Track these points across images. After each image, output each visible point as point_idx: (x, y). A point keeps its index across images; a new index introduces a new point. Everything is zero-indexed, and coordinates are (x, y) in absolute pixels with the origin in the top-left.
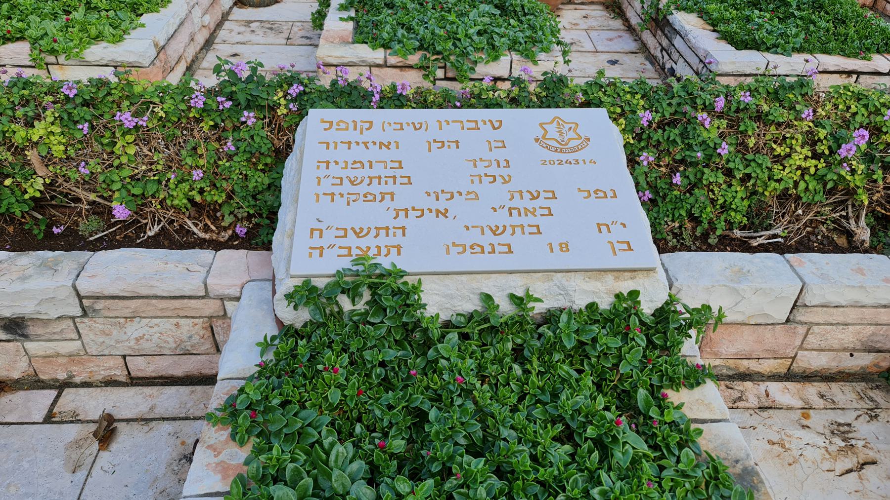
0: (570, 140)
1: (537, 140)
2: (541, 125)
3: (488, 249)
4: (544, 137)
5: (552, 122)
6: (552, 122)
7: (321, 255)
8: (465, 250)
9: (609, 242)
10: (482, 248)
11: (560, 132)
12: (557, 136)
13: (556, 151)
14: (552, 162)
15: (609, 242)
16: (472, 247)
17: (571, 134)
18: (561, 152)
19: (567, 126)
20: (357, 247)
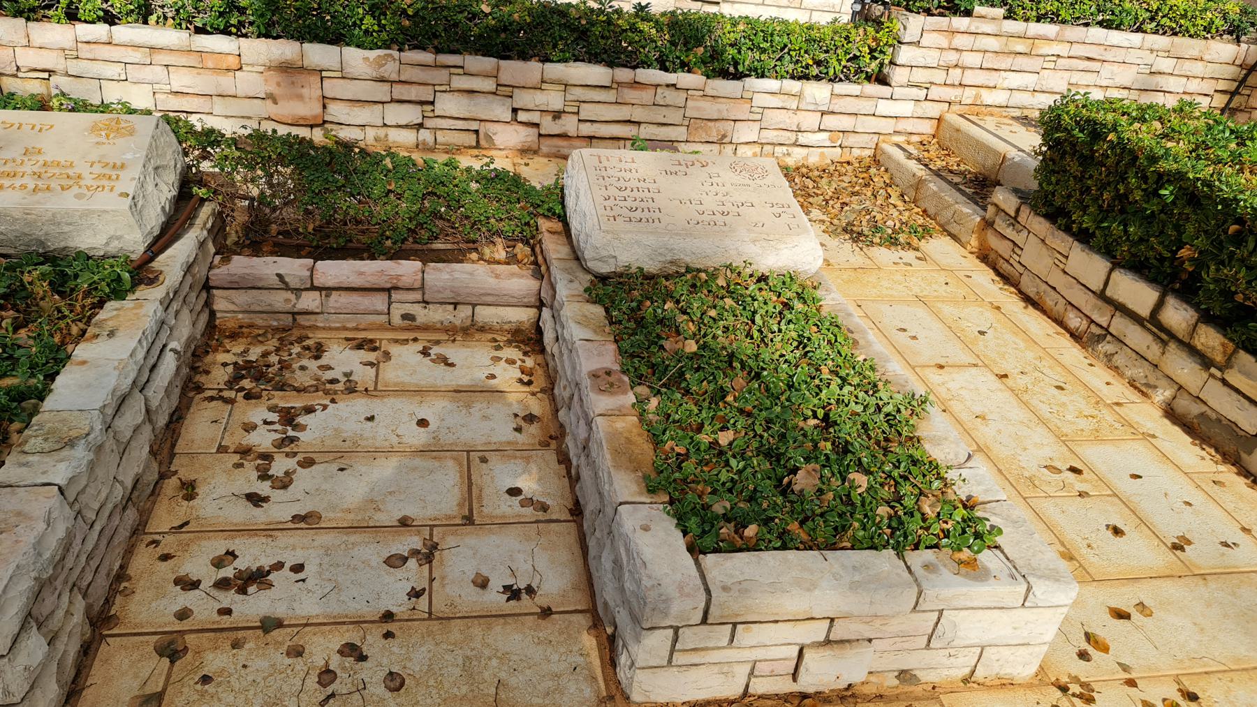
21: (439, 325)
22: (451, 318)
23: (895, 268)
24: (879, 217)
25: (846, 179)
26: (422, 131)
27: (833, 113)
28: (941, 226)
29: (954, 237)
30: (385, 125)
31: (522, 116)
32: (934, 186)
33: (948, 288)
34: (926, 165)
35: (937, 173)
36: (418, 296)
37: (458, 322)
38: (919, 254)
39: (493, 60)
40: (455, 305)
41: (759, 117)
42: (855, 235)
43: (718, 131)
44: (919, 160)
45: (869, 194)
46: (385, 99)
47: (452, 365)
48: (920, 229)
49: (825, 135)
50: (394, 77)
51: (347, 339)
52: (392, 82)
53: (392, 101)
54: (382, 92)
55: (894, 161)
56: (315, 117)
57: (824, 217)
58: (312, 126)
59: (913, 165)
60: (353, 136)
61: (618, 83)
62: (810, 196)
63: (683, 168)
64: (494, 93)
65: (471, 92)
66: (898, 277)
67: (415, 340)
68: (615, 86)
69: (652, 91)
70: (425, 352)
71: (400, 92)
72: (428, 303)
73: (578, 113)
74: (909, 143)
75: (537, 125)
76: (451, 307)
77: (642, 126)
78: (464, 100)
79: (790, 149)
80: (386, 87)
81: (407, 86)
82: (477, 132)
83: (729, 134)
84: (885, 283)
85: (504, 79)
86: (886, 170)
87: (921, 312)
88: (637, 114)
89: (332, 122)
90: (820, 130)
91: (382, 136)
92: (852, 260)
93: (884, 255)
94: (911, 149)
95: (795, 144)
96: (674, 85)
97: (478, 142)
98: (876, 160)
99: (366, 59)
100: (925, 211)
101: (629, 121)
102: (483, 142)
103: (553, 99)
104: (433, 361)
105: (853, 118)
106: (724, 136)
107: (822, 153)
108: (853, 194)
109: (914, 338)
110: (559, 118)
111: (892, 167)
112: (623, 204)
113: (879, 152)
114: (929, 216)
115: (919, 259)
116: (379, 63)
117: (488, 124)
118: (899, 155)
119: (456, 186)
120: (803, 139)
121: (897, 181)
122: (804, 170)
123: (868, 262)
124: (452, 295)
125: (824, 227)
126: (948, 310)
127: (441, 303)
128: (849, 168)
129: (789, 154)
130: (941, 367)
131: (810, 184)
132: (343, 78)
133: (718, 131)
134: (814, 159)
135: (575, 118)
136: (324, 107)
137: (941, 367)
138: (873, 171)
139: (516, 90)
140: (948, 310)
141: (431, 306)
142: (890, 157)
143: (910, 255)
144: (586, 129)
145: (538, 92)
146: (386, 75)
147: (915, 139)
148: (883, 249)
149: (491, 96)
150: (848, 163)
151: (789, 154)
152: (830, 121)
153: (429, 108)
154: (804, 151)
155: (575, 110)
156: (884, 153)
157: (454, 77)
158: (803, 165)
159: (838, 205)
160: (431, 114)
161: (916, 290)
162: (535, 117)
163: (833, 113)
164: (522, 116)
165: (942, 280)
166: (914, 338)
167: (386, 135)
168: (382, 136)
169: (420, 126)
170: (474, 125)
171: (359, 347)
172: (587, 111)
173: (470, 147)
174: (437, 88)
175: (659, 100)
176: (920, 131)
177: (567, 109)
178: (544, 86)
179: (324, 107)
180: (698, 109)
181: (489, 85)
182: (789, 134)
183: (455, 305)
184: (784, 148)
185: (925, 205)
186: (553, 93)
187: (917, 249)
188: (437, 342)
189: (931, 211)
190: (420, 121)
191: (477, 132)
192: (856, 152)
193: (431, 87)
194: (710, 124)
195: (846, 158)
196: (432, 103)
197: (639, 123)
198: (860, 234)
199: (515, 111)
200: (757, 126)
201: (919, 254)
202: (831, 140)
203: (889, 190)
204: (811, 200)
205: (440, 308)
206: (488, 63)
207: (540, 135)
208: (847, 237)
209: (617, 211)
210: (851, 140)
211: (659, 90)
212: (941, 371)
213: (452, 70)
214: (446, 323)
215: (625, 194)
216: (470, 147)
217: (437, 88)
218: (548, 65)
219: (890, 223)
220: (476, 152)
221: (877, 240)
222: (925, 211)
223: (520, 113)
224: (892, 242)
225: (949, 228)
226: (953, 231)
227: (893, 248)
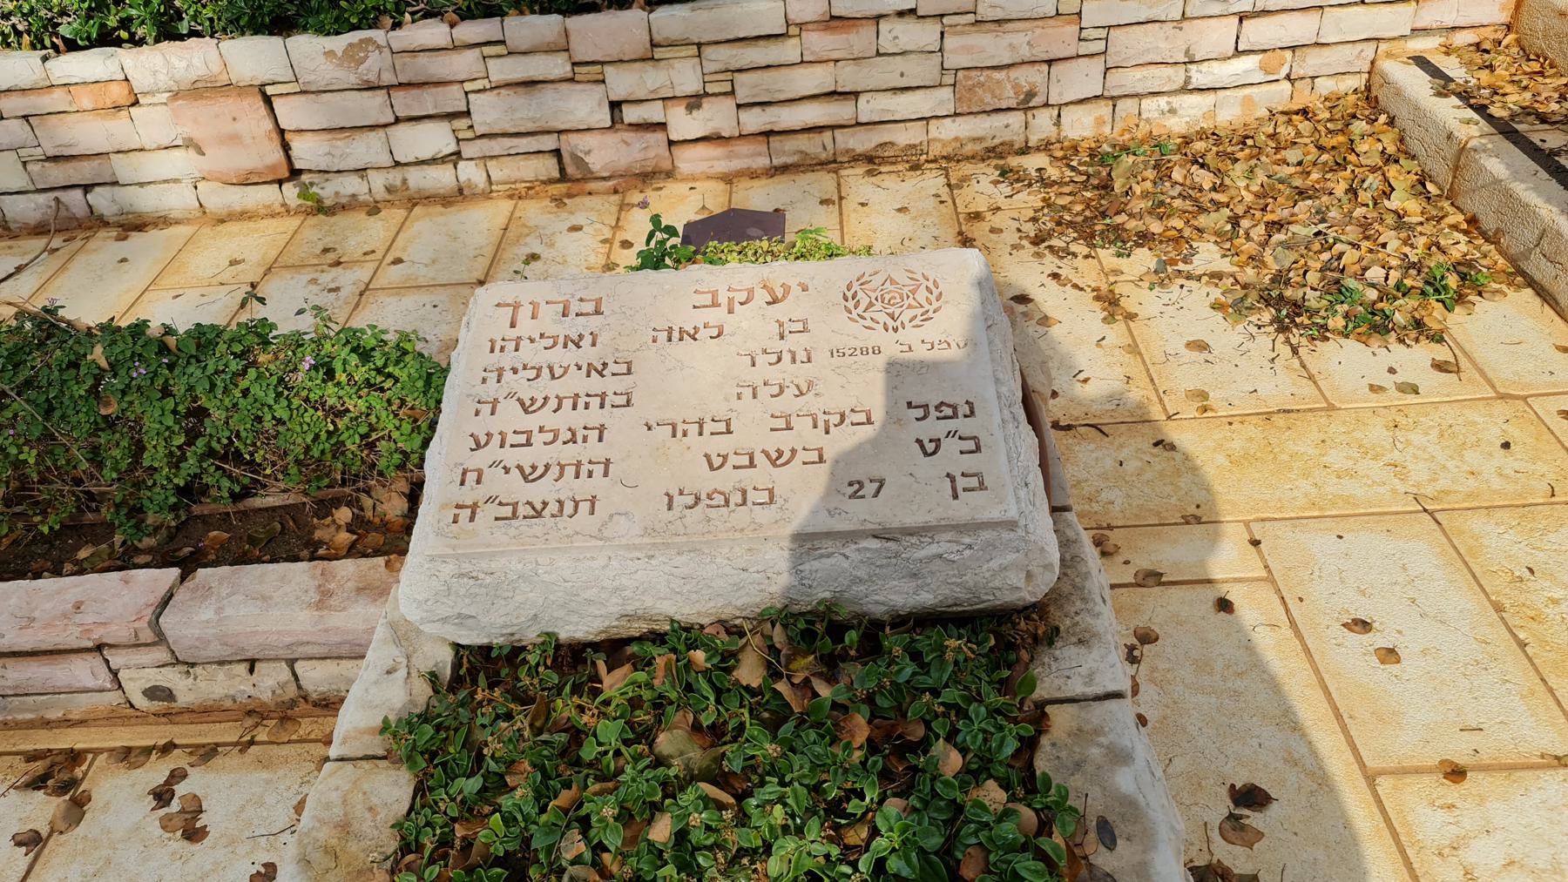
3: (736, 498)
9: (948, 475)
15: (948, 475)
20: (528, 503)
21: (228, 704)
22: (251, 691)
23: (1375, 400)
24: (1350, 256)
25: (1292, 155)
26: (461, 164)
27: (1266, 13)
28: (1512, 260)
29: (1544, 295)
30: (397, 164)
31: (631, 114)
32: (1500, 164)
33: (1509, 462)
34: (1481, 109)
35: (1506, 130)
36: (161, 655)
37: (266, 697)
38: (1441, 353)
39: (555, 18)
40: (252, 664)
41: (1100, 46)
42: (1288, 314)
43: (1016, 86)
44: (1465, 96)
45: (1340, 189)
46: (383, 121)
47: (194, 834)
48: (1452, 281)
49: (1250, 62)
50: (388, 78)
51: (32, 757)
52: (389, 87)
53: (398, 120)
54: (373, 107)
55: (1407, 100)
56: (273, 168)
57: (1225, 265)
58: (280, 182)
59: (1450, 112)
60: (350, 190)
61: (800, 25)
62: (1202, 210)
63: (716, 316)
64: (572, 80)
65: (530, 84)
66: (1377, 432)
67: (168, 748)
68: (793, 30)
69: (868, 31)
70: (162, 796)
71: (406, 103)
72: (193, 665)
73: (732, 93)
74: (1448, 51)
75: (662, 126)
76: (242, 669)
77: (862, 99)
78: (517, 99)
79: (1177, 101)
80: (380, 96)
81: (415, 92)
82: (557, 153)
83: (1042, 89)
84: (1336, 458)
85: (582, 51)
86: (1391, 122)
87: (1421, 552)
88: (848, 78)
89: (310, 171)
90: (1238, 53)
91: (398, 183)
92: (1266, 388)
93: (1348, 362)
94: (1453, 68)
95: (1185, 89)
96: (913, 11)
97: (562, 170)
98: (1370, 98)
99: (330, 54)
100: (1472, 220)
101: (834, 93)
102: (570, 170)
103: (686, 77)
104: (166, 824)
105: (1314, 17)
106: (1031, 95)
107: (1248, 102)
108: (1302, 193)
109: (1389, 655)
110: (699, 106)
111: (1403, 114)
112: (511, 457)
113: (1376, 79)
114: (1483, 234)
115: (1440, 366)
116: (352, 56)
117: (573, 138)
118: (1417, 84)
119: (245, 393)
120: (1199, 76)
121: (1415, 146)
122: (1199, 146)
123: (1307, 389)
124: (229, 651)
125: (1216, 293)
126: (1500, 542)
127: (221, 663)
128: (1305, 127)
129: (1172, 111)
130: (1456, 773)
131: (1205, 179)
132: (302, 92)
133: (1016, 86)
134: (1229, 113)
135: (729, 104)
136: (286, 147)
137: (1456, 773)
138: (1359, 126)
139: (608, 70)
140: (1500, 542)
141: (198, 670)
142: (1398, 93)
143: (1415, 359)
144: (754, 120)
145: (648, 66)
146: (372, 77)
147: (1463, 39)
148: (1351, 344)
149: (565, 86)
150: (1304, 112)
151: (1172, 111)
152: (1257, 32)
153: (462, 123)
154: (1210, 98)
155: (727, 87)
156: (1383, 76)
157: (490, 62)
158: (1202, 135)
159: (1261, 229)
160: (470, 134)
161: (1419, 472)
162: (653, 113)
163: (1266, 13)
164: (631, 114)
165: (1495, 436)
166: (1389, 655)
167: (405, 181)
168: (398, 183)
169: (458, 155)
170: (549, 143)
171: (37, 783)
172: (747, 86)
173: (551, 181)
174: (468, 86)
175: (886, 45)
176: (1476, 20)
177: (710, 89)
178: (659, 53)
179: (286, 147)
180: (968, 50)
181: (557, 66)
182: (1169, 70)
183: (252, 664)
184: (1162, 101)
185: (1474, 205)
186: (677, 64)
187: (1437, 338)
188: (207, 753)
189: (1489, 223)
190: (452, 148)
191: (557, 153)
192: (1325, 86)
193: (456, 87)
194: (997, 75)
195: (1304, 98)
196: (468, 114)
197: (856, 94)
198: (1298, 307)
199: (615, 106)
200: (1097, 65)
201: (1441, 353)
202: (1264, 68)
203: (1392, 171)
204: (1203, 221)
205: (221, 673)
206: (546, 26)
207: (671, 143)
208: (1267, 316)
209: (497, 484)
210: (1312, 62)
211: (884, 26)
212: (1452, 792)
213: (487, 50)
214: (242, 699)
215: (531, 422)
216: (551, 181)
217: (468, 86)
218: (663, 13)
219: (1376, 273)
220: (561, 188)
221: (1337, 322)
222: (1472, 220)
223: (624, 107)
224: (1374, 325)
225: (1530, 268)
226: (1538, 276)
227: (1375, 341)
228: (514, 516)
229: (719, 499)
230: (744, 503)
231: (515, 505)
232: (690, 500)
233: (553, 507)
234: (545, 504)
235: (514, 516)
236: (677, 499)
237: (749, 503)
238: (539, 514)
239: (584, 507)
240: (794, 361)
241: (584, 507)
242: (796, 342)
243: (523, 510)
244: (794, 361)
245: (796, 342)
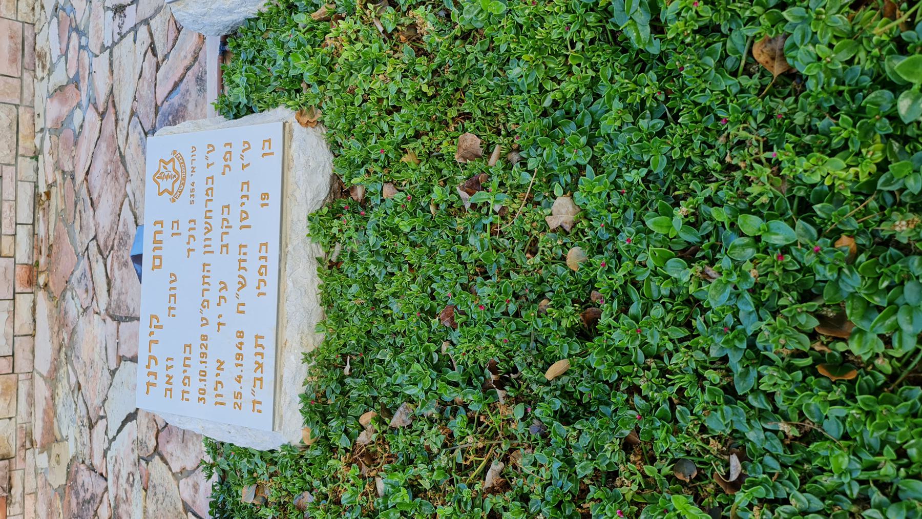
0: (174, 169)
1: (173, 201)
2: (160, 194)
3: (263, 262)
4: (170, 193)
5: (158, 184)
6: (158, 184)
7: (260, 403)
8: (263, 281)
10: (262, 266)
11: (168, 177)
12: (171, 181)
13: (183, 184)
14: (192, 190)
16: (261, 274)
17: (170, 167)
18: (184, 179)
19: (162, 170)
228: (261, 379)
229: (263, 270)
230: (265, 258)
231: (256, 379)
232: (262, 284)
233: (259, 358)
234: (256, 362)
235: (261, 379)
236: (261, 291)
237: (265, 255)
238: (260, 366)
239: (260, 341)
240: (194, 229)
241: (260, 341)
242: (184, 227)
243: (258, 375)
244: (194, 229)
245: (184, 227)
